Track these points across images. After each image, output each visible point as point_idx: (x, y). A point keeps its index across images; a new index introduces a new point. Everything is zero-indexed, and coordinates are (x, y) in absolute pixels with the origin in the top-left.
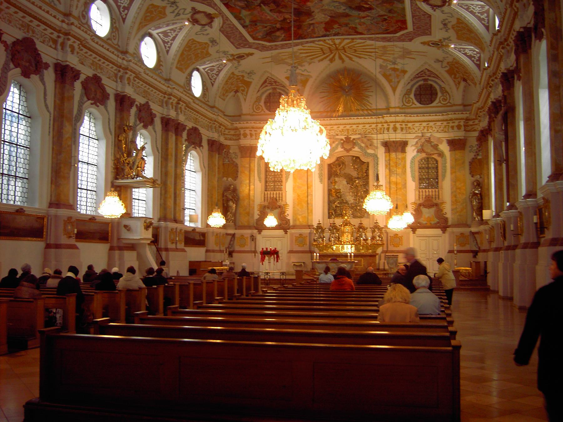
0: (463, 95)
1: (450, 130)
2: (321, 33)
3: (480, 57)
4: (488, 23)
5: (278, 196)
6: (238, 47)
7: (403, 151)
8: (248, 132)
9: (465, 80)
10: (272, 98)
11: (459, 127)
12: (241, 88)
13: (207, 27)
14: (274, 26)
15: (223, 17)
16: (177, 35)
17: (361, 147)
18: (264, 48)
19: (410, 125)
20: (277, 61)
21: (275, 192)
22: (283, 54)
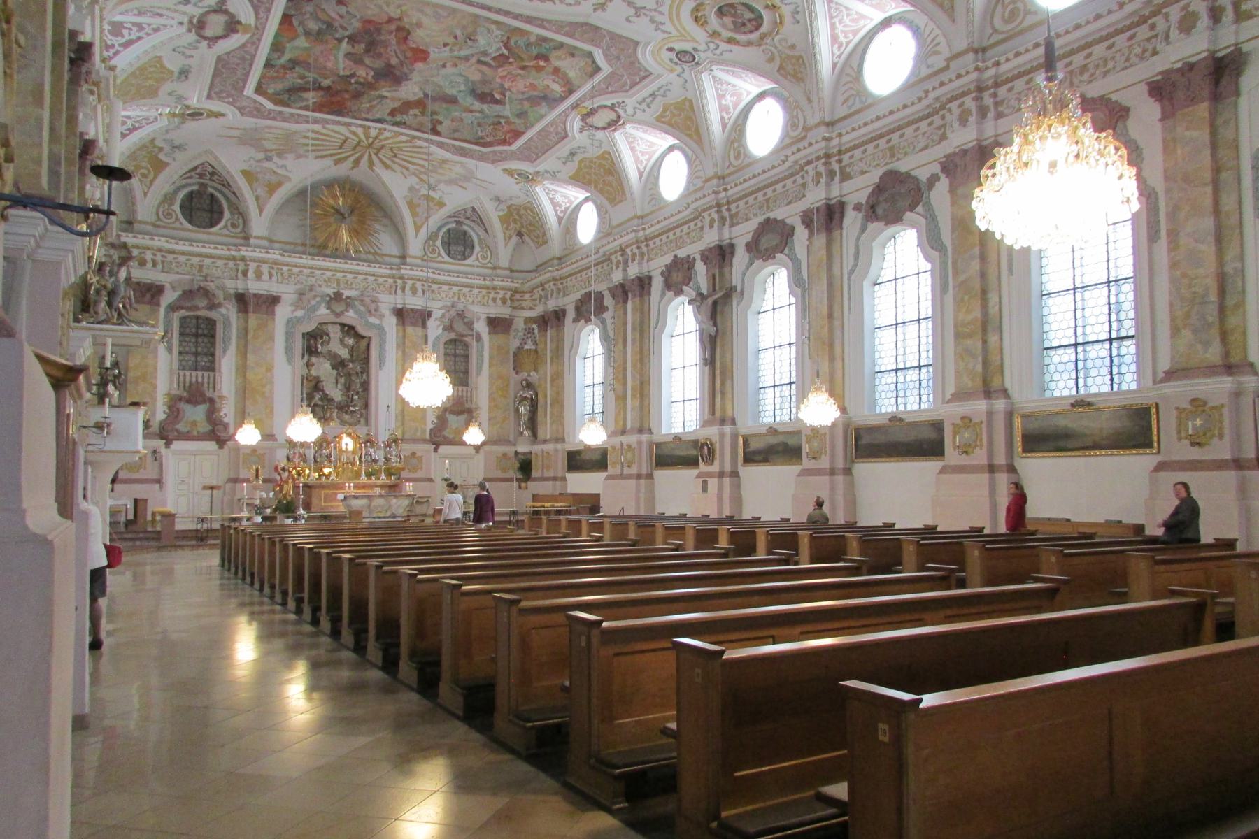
0: (512, 256)
1: (490, 301)
2: (378, 116)
3: (567, 209)
4: (645, 168)
5: (206, 380)
6: (213, 95)
7: (424, 326)
8: (148, 256)
9: (520, 234)
10: (195, 200)
11: (504, 301)
12: (142, 171)
13: (205, 43)
14: (320, 80)
15: (251, 37)
16: (140, 38)
17: (356, 312)
18: (258, 112)
19: (435, 287)
20: (249, 139)
21: (200, 374)
22: (273, 131)
